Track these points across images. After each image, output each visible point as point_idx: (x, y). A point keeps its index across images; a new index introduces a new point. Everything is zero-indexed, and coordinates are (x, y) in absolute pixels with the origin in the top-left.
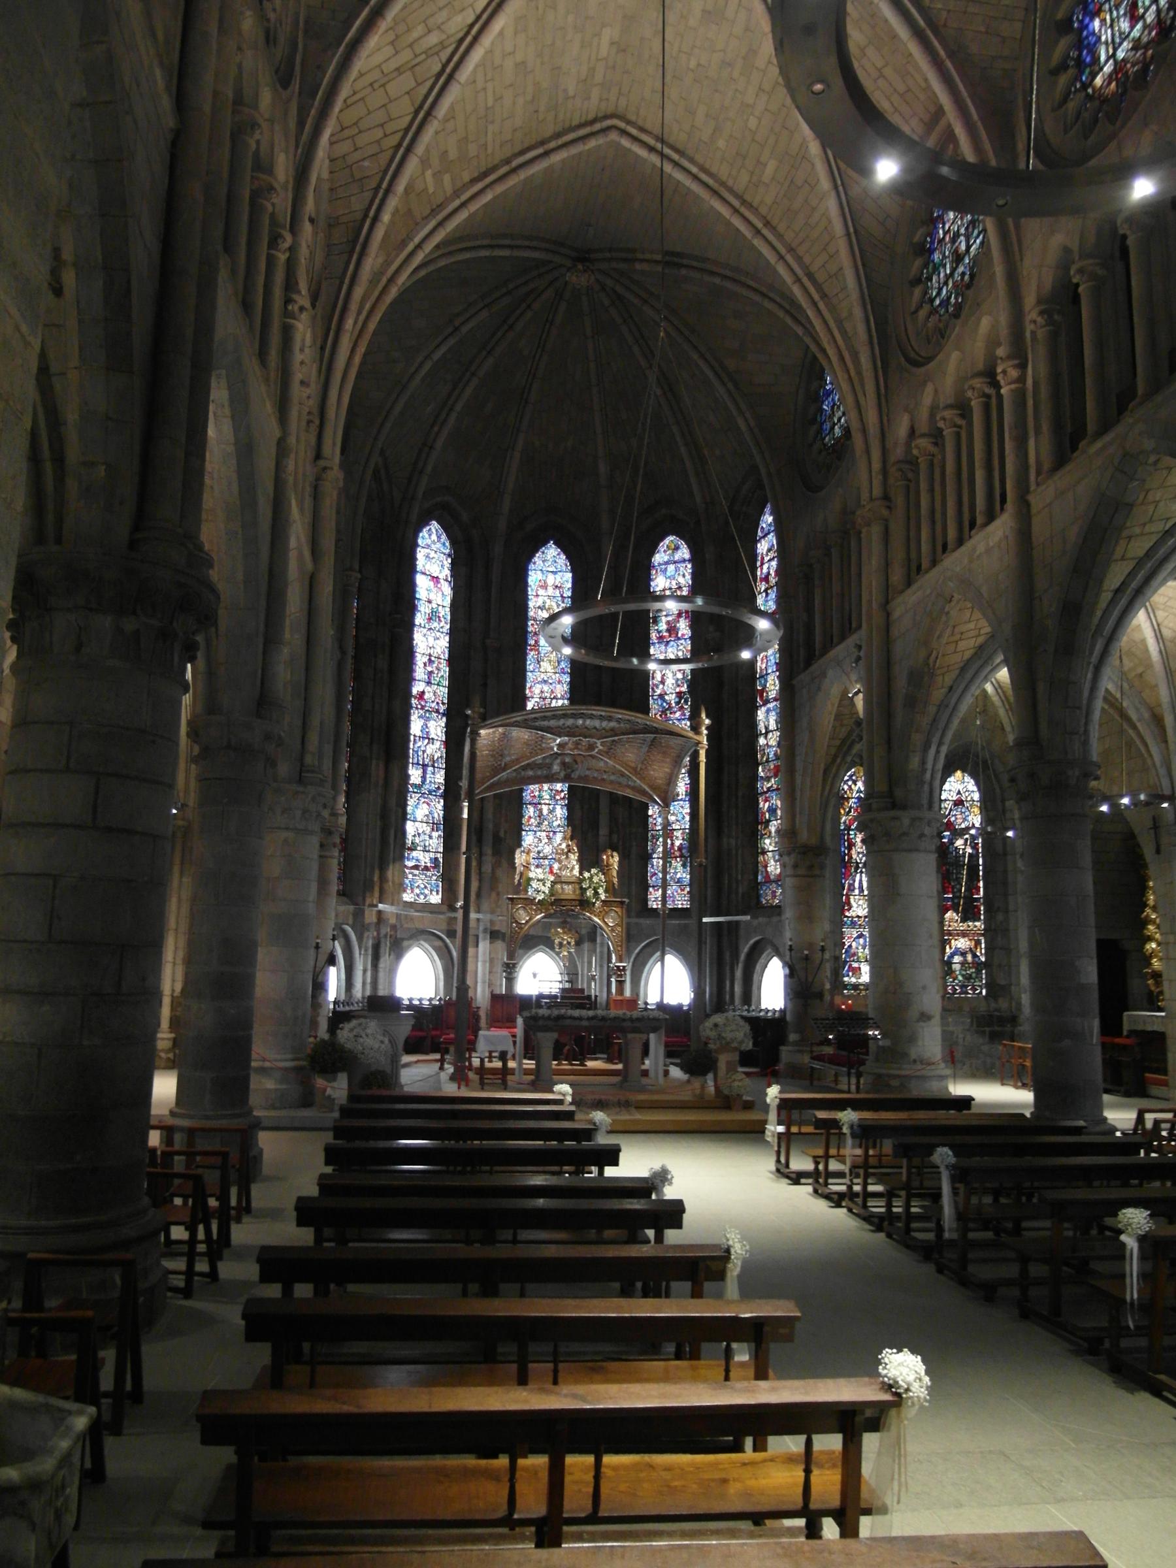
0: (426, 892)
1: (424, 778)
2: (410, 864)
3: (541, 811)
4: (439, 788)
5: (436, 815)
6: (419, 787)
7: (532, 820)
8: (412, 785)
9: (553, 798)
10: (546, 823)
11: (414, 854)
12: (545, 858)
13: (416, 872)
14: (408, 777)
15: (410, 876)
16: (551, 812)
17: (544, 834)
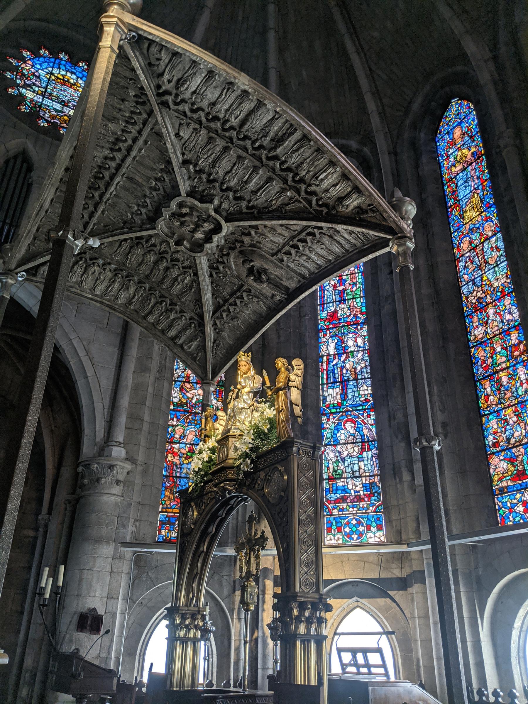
0: (361, 529)
1: (344, 395)
2: (333, 497)
3: (499, 381)
4: (367, 400)
5: (366, 432)
6: (339, 405)
7: (491, 398)
8: (328, 406)
9: (510, 357)
10: (509, 394)
11: (340, 484)
12: (519, 444)
13: (344, 505)
14: (325, 399)
15: (335, 512)
16: (511, 377)
17: (509, 411)
